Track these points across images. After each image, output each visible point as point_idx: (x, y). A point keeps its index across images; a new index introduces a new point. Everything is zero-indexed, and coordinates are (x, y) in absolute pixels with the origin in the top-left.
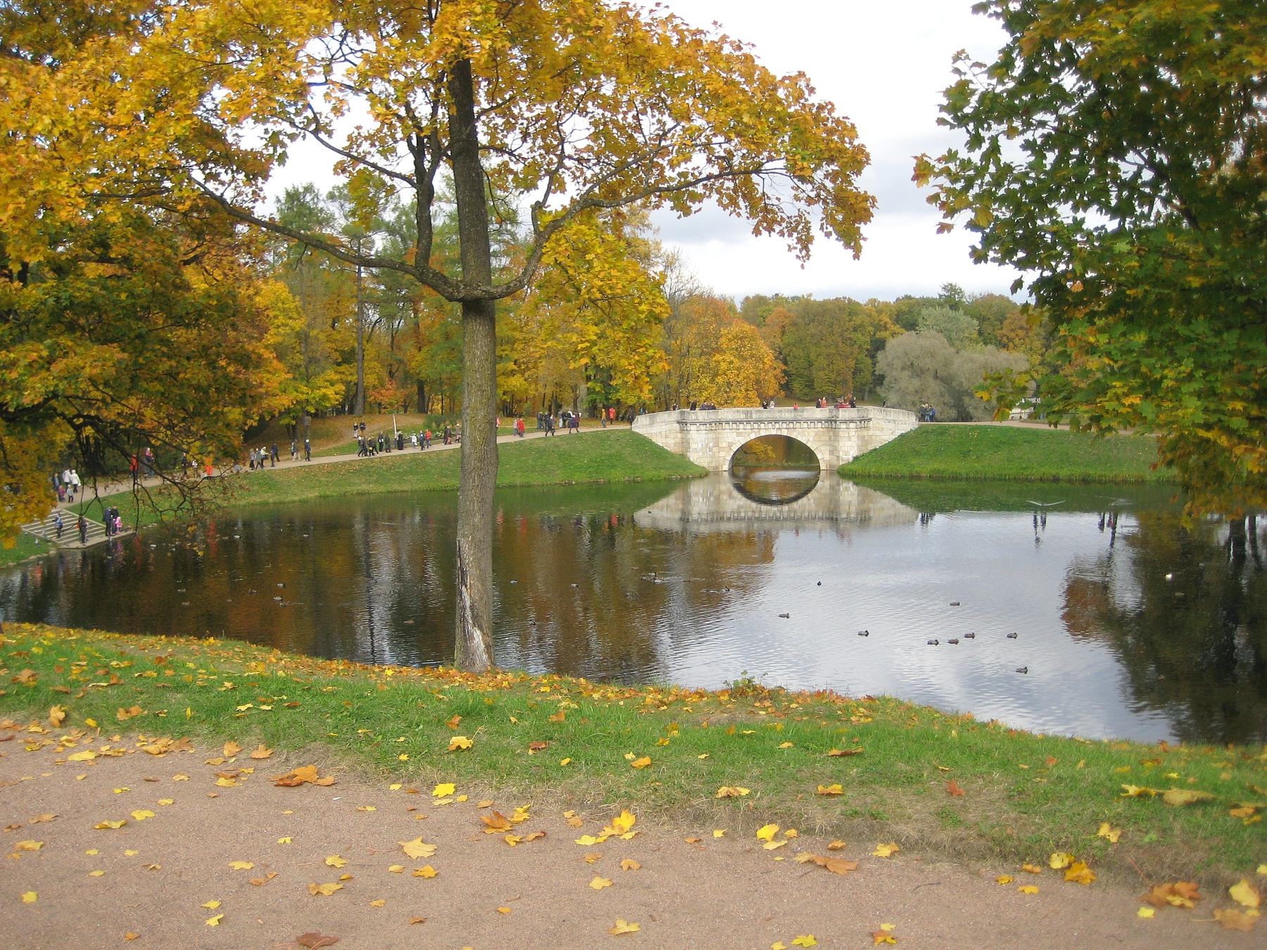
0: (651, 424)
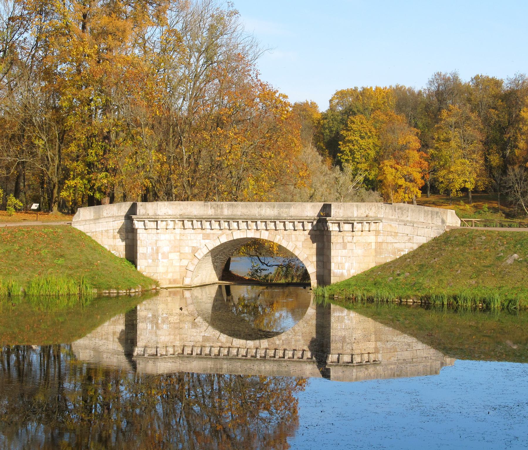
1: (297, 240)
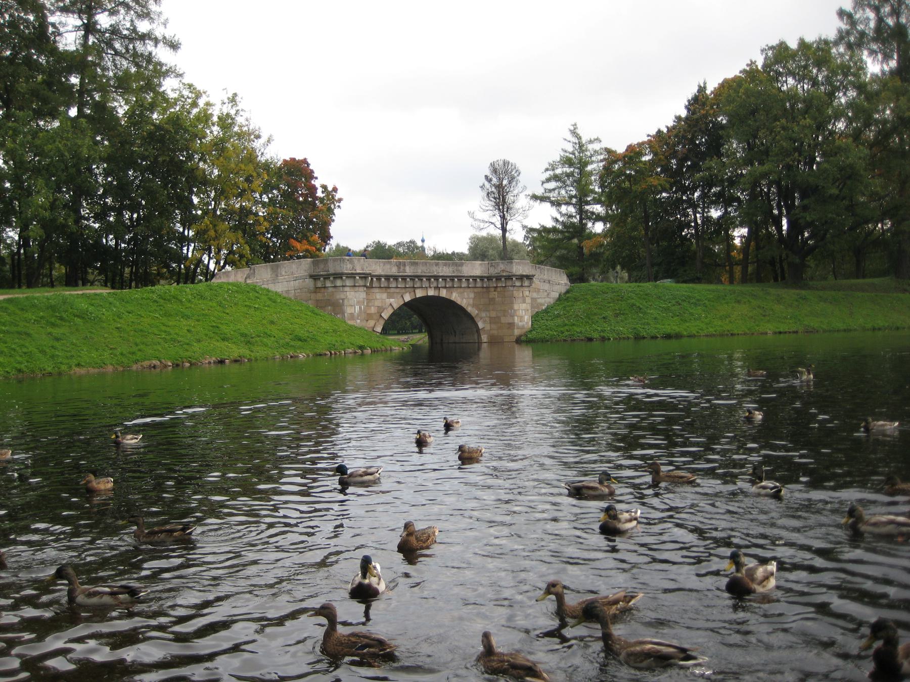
0: (274, 281)
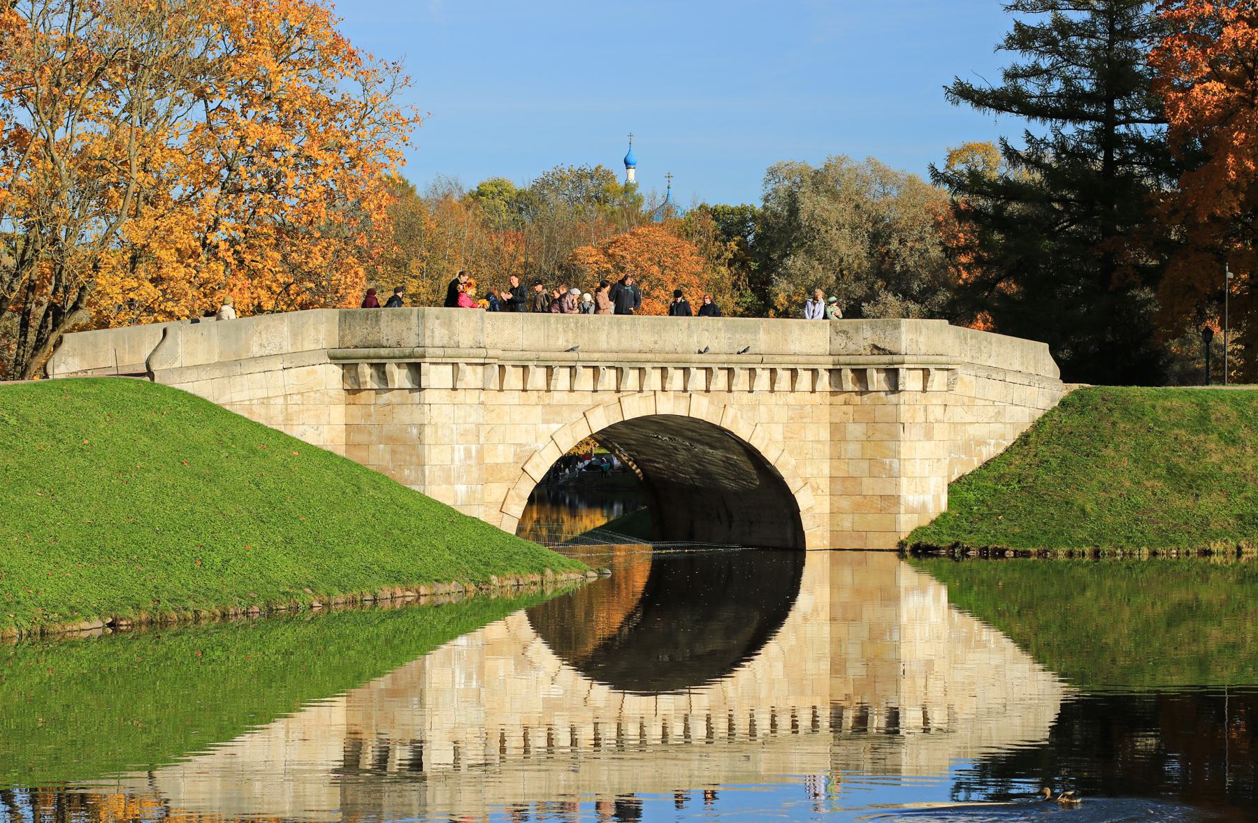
0: (232, 364)
1: (771, 421)
